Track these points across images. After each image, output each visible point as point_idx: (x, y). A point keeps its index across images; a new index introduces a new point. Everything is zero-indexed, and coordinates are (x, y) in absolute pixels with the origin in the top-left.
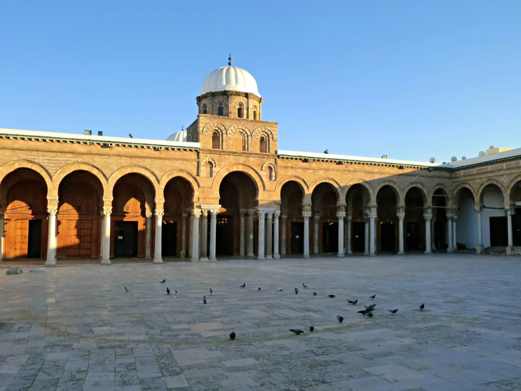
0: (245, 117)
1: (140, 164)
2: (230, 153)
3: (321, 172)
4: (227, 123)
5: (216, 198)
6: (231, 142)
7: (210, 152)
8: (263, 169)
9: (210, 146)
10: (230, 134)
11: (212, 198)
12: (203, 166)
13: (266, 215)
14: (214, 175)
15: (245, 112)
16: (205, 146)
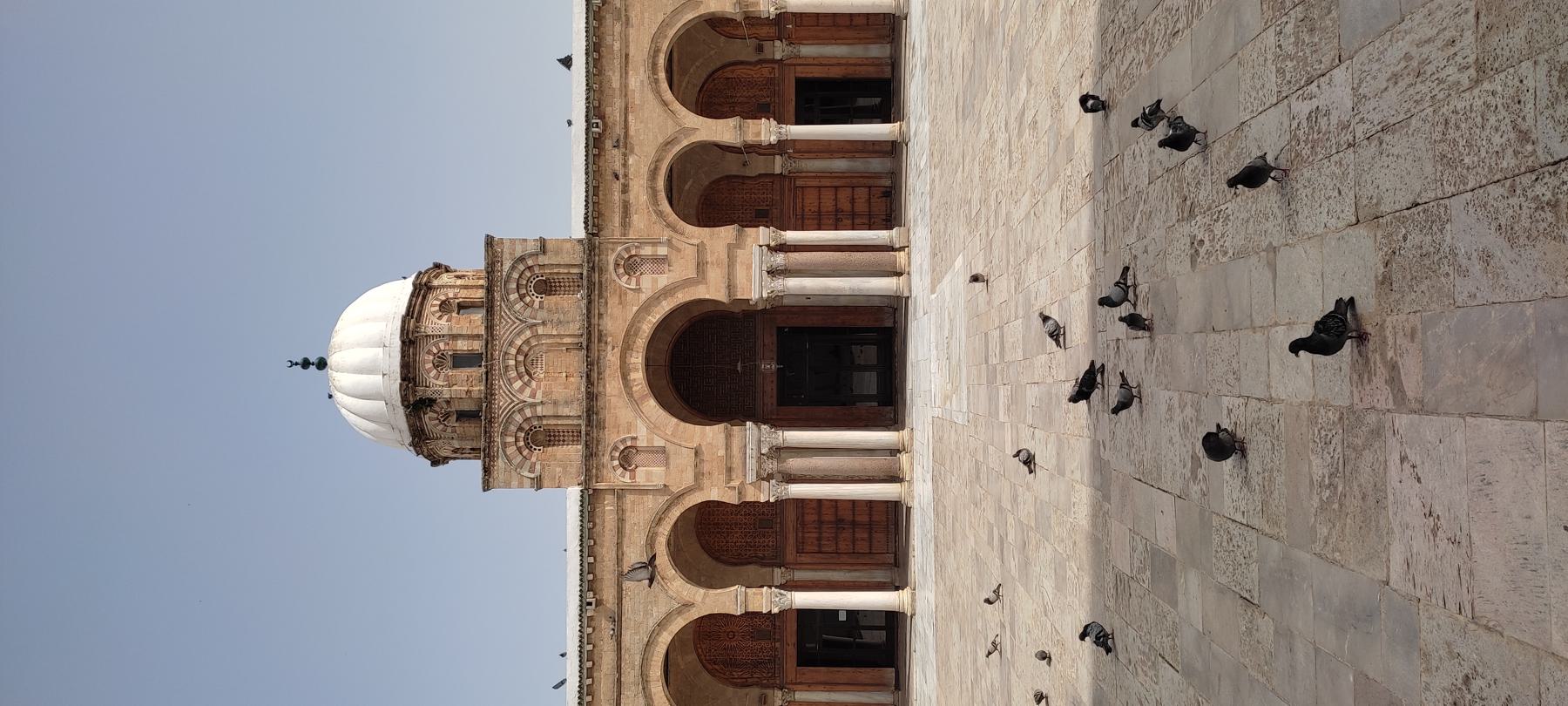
0: (477, 346)
1: (638, 660)
2: (592, 397)
3: (633, 82)
4: (502, 402)
5: (728, 437)
6: (559, 392)
7: (591, 454)
8: (633, 286)
9: (572, 453)
10: (533, 395)
11: (728, 447)
12: (633, 477)
13: (773, 273)
14: (659, 442)
15: (462, 346)
16: (573, 470)
